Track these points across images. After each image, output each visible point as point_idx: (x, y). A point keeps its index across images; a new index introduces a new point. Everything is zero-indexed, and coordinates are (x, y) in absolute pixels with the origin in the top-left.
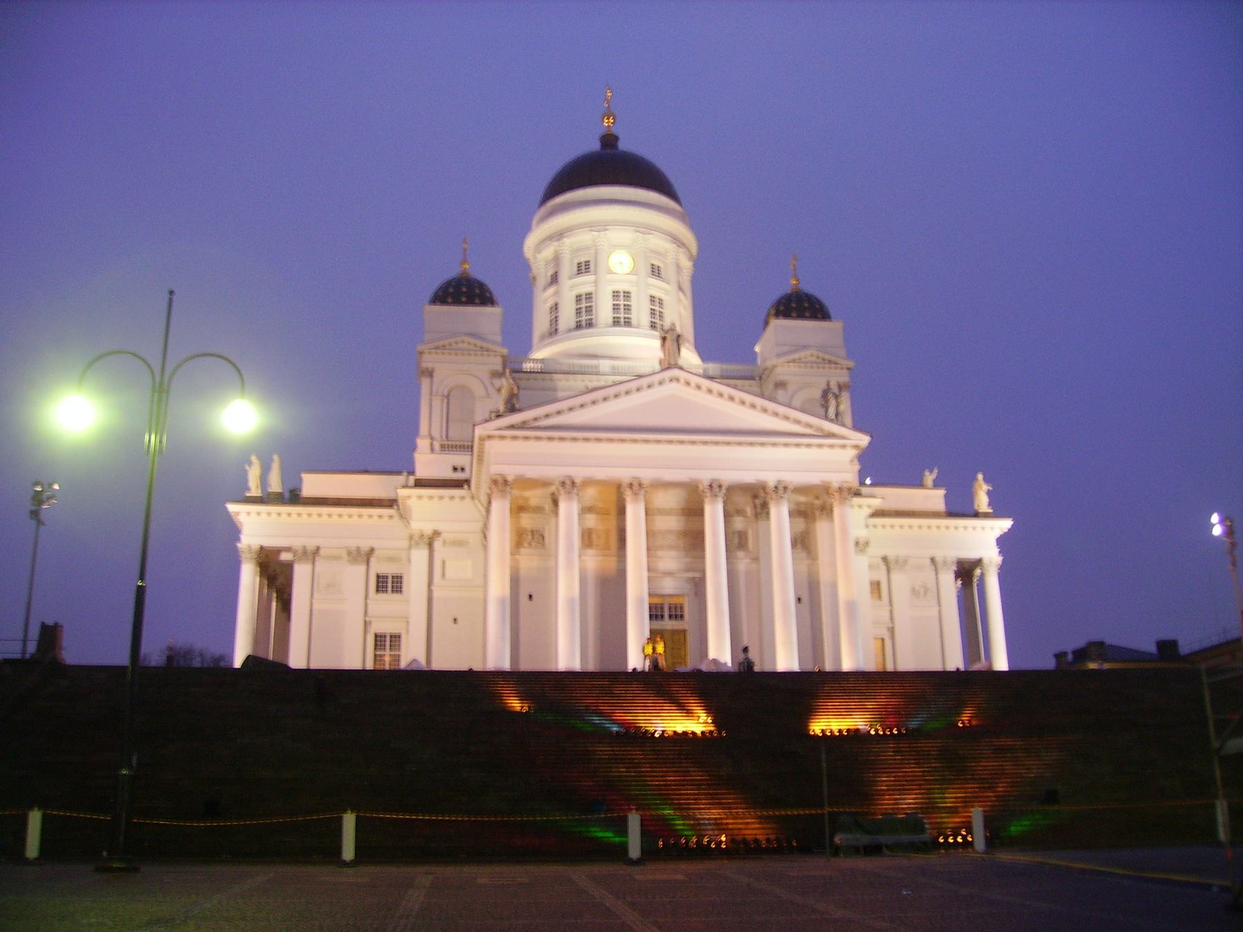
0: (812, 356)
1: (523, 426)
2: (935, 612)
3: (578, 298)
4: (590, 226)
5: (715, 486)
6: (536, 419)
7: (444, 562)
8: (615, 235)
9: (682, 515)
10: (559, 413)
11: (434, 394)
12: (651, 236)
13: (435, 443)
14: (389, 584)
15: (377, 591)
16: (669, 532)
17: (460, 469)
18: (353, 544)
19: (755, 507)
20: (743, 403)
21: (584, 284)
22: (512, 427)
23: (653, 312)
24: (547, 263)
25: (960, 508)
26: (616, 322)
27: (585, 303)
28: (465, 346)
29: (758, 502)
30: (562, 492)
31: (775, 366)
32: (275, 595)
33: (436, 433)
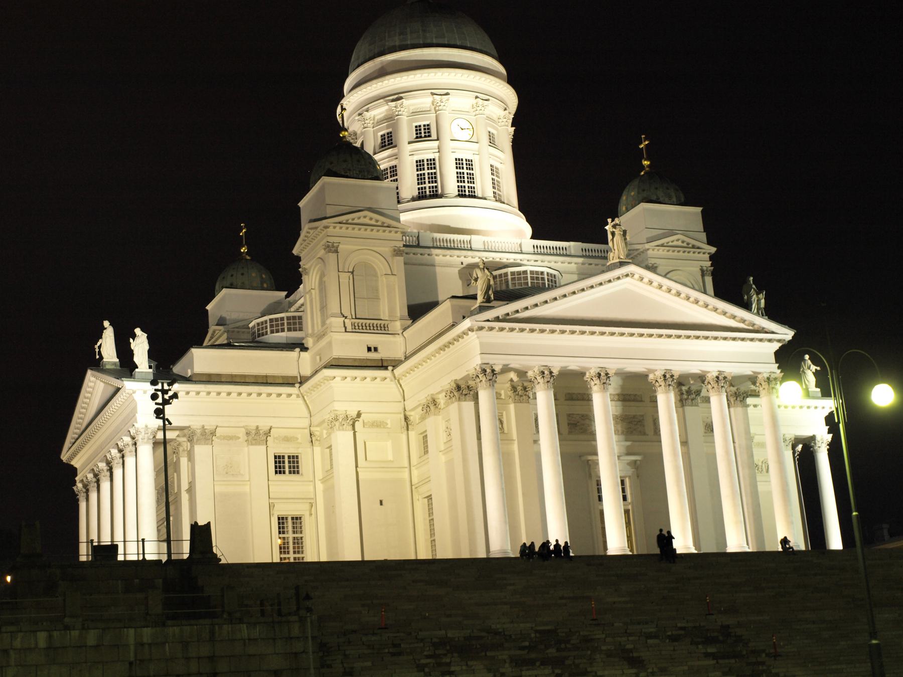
0: (678, 240)
1: (506, 319)
3: (420, 164)
5: (668, 376)
6: (517, 311)
9: (619, 400)
11: (340, 270)
13: (346, 320)
15: (276, 472)
18: (252, 423)
20: (688, 298)
21: (427, 150)
22: (497, 319)
28: (367, 221)
29: (684, 388)
31: (648, 249)
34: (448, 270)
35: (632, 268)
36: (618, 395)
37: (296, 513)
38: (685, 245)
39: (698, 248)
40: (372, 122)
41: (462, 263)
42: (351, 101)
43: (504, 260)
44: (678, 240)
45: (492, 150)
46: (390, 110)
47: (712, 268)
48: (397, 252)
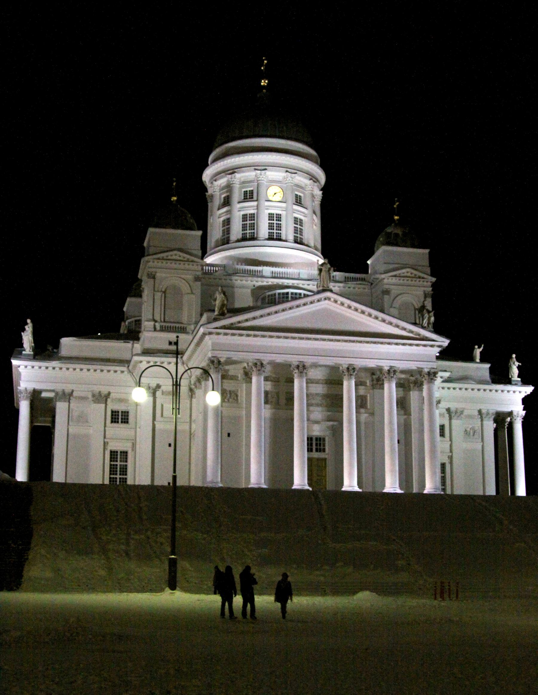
2: (480, 447)
3: (245, 217)
4: (256, 167)
5: (350, 368)
6: (239, 322)
7: (162, 406)
8: (272, 174)
9: (326, 383)
11: (156, 290)
12: (296, 175)
13: (157, 324)
15: (112, 422)
16: (317, 394)
17: (173, 343)
18: (96, 389)
19: (373, 381)
22: (224, 327)
23: (296, 230)
26: (271, 238)
29: (374, 377)
30: (254, 369)
31: (384, 279)
33: (157, 317)
34: (244, 290)
35: (328, 294)
36: (326, 380)
37: (125, 449)
38: (413, 275)
39: (423, 278)
40: (219, 188)
41: (254, 286)
42: (207, 175)
43: (286, 284)
44: (408, 272)
45: (296, 207)
46: (228, 181)
47: (432, 292)
48: (197, 279)
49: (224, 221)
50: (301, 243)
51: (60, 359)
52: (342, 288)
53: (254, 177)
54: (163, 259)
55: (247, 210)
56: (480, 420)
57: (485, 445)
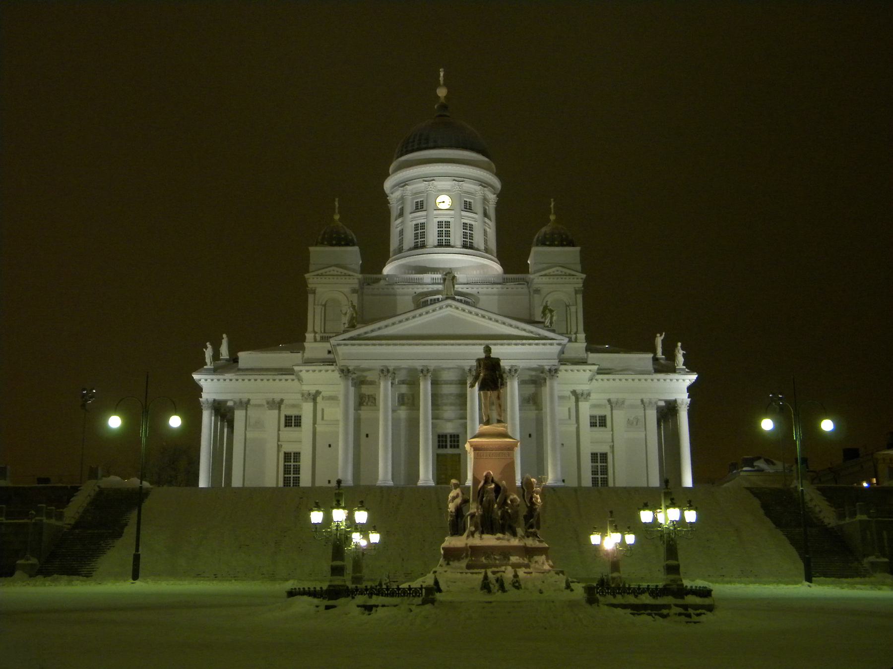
0: (558, 271)
6: (366, 333)
7: (323, 410)
9: (459, 384)
10: (379, 329)
13: (317, 335)
14: (293, 421)
15: (286, 426)
16: (451, 394)
18: (270, 396)
23: (465, 235)
24: (398, 201)
25: (666, 367)
26: (440, 245)
27: (420, 229)
28: (335, 273)
31: (534, 279)
32: (226, 424)
33: (317, 329)
36: (459, 380)
38: (563, 273)
39: (573, 275)
40: (396, 200)
41: (415, 293)
44: (558, 271)
45: (464, 213)
49: (400, 231)
50: (471, 247)
51: (239, 370)
52: (500, 289)
53: (424, 188)
54: (322, 275)
55: (417, 220)
56: (643, 409)
57: (647, 433)
